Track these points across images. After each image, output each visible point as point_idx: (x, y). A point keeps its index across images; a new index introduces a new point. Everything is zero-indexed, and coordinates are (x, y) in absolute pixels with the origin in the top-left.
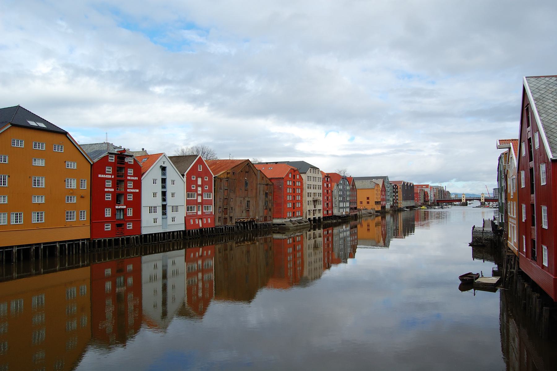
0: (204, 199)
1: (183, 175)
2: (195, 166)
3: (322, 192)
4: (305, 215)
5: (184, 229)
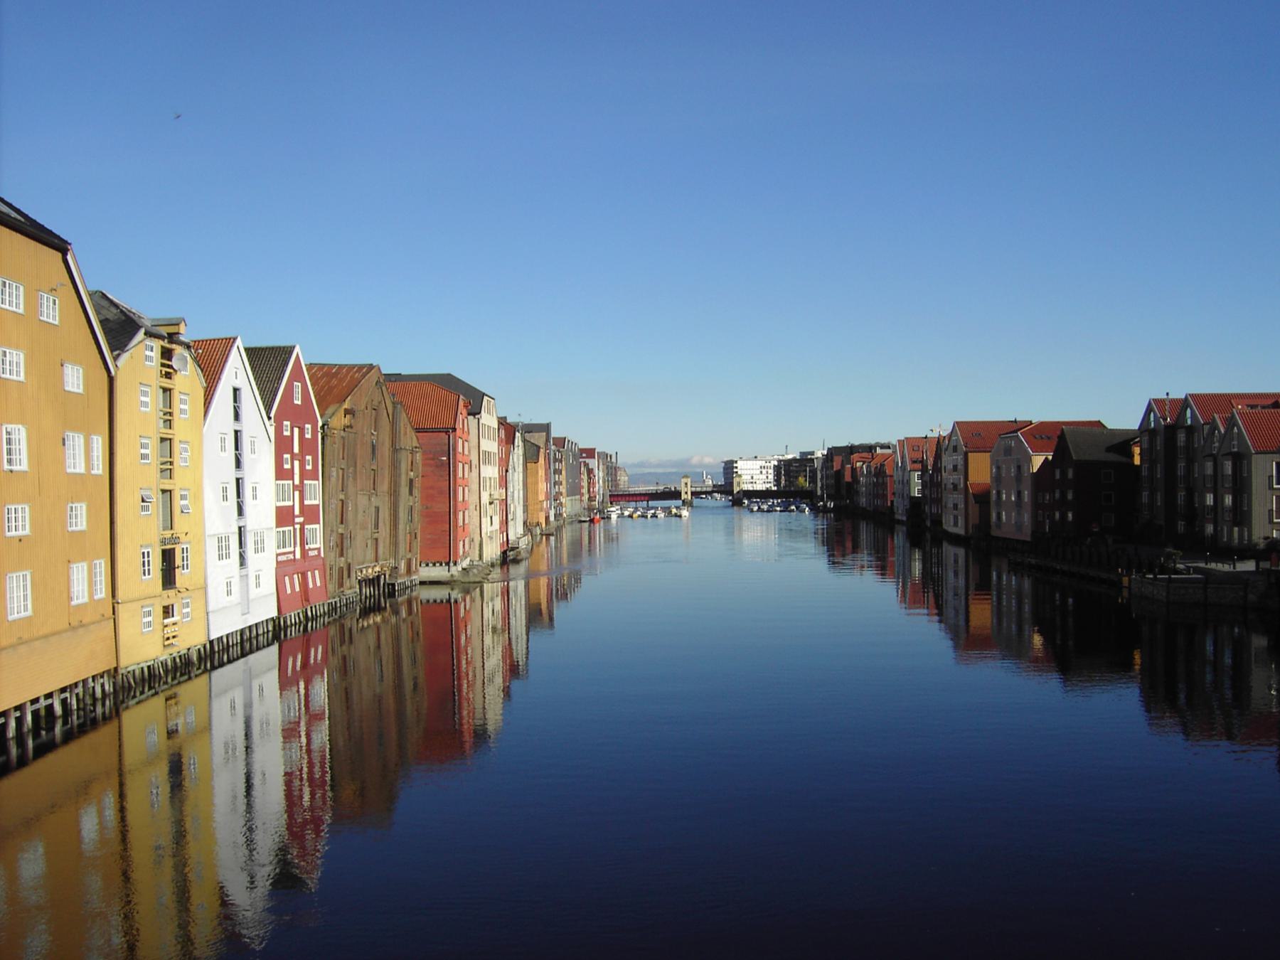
0: (306, 502)
1: (269, 418)
4: (477, 552)
5: (274, 614)
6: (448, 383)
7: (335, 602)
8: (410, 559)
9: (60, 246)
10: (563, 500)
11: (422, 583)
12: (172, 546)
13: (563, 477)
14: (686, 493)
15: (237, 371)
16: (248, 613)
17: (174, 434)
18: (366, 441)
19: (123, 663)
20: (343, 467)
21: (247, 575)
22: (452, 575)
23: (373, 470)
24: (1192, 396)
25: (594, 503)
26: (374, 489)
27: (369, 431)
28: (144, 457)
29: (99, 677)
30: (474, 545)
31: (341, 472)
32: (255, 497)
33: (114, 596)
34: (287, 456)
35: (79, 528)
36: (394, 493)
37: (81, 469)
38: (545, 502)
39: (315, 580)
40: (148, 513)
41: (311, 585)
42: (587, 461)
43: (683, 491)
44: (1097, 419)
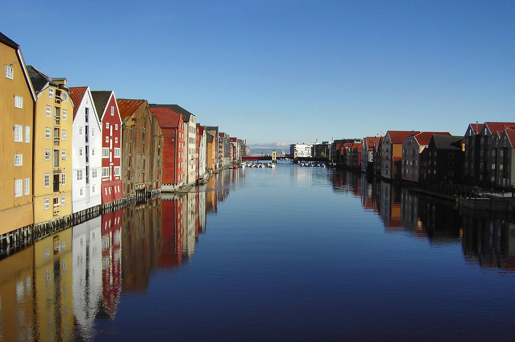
0: (115, 157)
1: (100, 121)
2: (109, 109)
3: (195, 148)
5: (100, 203)
6: (176, 108)
7: (126, 199)
8: (158, 182)
9: (15, 46)
10: (222, 159)
11: (162, 192)
12: (58, 174)
13: (223, 150)
14: (274, 157)
15: (87, 101)
16: (89, 202)
17: (60, 127)
18: (141, 132)
19: (36, 222)
20: (130, 142)
21: (89, 187)
22: (175, 189)
23: (143, 144)
24: (487, 123)
25: (235, 160)
26: (143, 152)
27: (142, 127)
28: (47, 136)
29: (26, 228)
30: (185, 177)
31: (130, 144)
32: (93, 154)
33: (33, 194)
34: (107, 137)
35: (19, 165)
36: (152, 154)
37: (21, 140)
38: (215, 160)
39: (117, 189)
40: (48, 159)
41: (116, 192)
42: (233, 143)
43: (273, 156)
44: (447, 132)
